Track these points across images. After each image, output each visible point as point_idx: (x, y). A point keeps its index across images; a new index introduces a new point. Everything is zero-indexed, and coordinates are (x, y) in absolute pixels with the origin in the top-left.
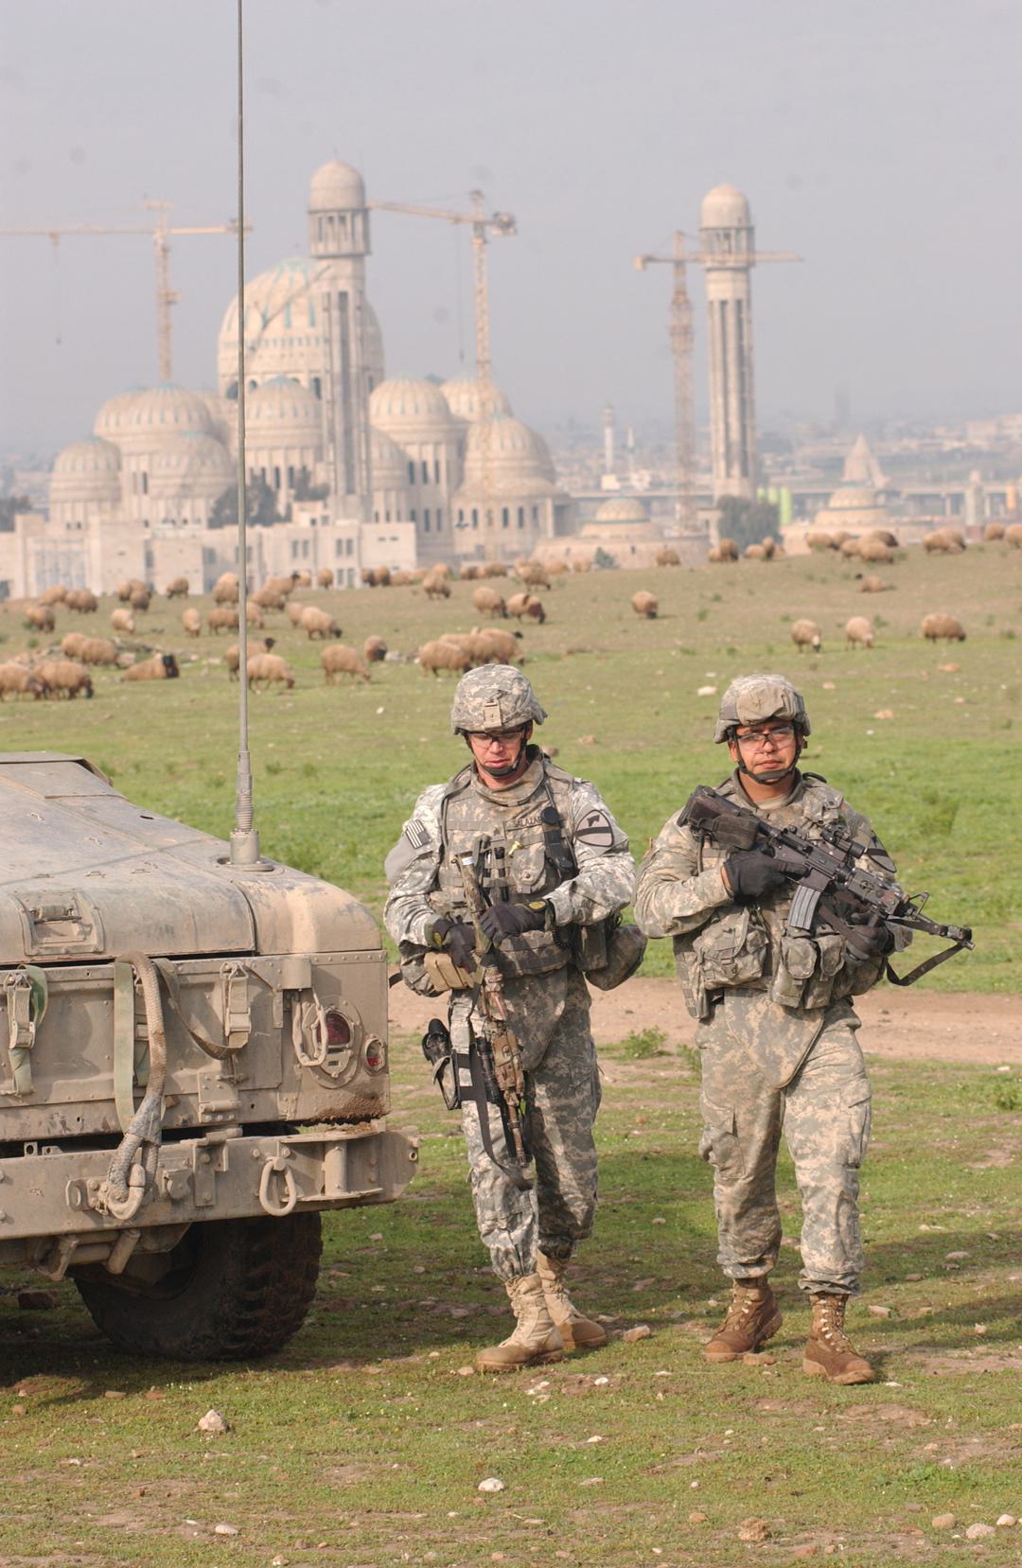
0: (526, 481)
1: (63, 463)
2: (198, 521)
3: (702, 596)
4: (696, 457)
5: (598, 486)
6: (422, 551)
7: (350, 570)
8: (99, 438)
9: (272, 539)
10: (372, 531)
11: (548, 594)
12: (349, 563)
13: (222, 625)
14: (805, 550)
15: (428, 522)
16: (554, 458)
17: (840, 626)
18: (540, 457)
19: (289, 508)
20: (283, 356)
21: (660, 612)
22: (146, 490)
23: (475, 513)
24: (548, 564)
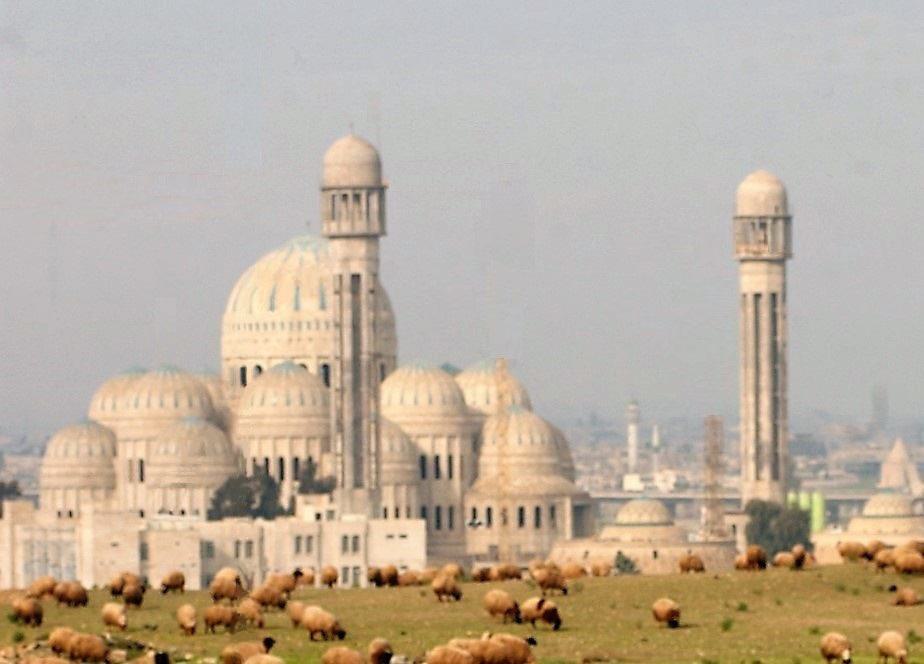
0: (545, 479)
1: (56, 447)
2: (197, 512)
3: (727, 606)
4: (725, 458)
5: (620, 486)
6: (432, 550)
7: (356, 568)
8: (94, 423)
9: (275, 530)
10: (380, 527)
11: (565, 599)
12: (353, 560)
13: (219, 622)
14: (838, 560)
15: (439, 520)
16: (574, 455)
17: (872, 640)
18: (560, 454)
19: (293, 501)
20: (290, 340)
21: (682, 620)
22: (142, 479)
23: (489, 511)
24: (565, 567)
